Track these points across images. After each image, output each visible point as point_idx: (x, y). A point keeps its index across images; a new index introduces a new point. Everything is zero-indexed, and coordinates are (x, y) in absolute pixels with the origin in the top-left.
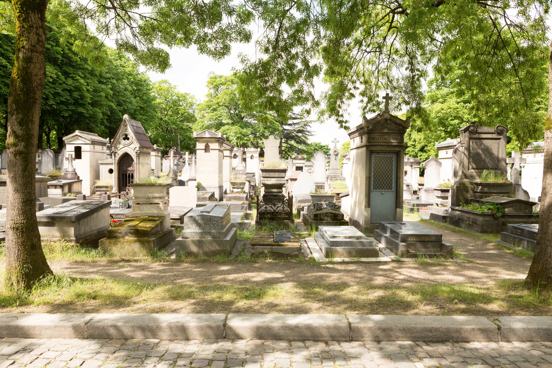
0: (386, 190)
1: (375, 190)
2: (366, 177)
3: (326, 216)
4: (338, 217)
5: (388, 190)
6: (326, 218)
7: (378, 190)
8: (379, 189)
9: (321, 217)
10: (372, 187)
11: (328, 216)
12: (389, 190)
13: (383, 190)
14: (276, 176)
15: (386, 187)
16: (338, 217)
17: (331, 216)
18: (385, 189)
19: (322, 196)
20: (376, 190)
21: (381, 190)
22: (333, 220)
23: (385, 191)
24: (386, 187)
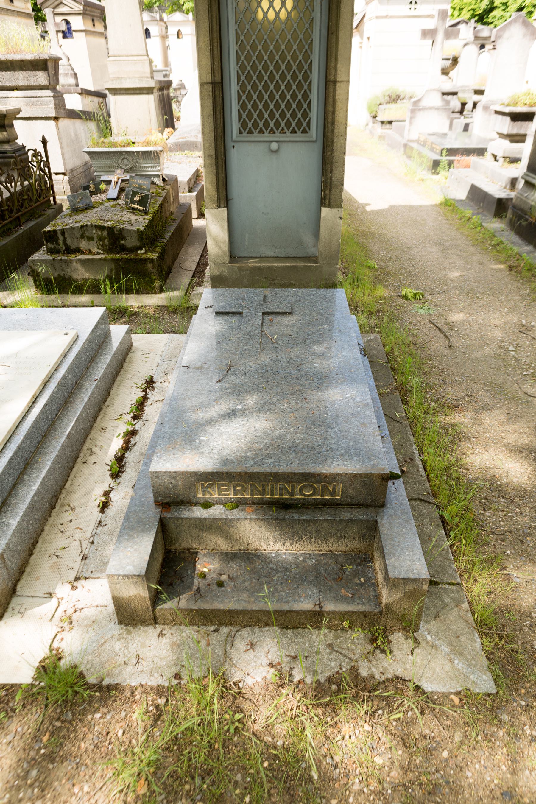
0: (289, 137)
1: (245, 137)
2: (202, 85)
3: (82, 237)
4: (124, 238)
5: (294, 137)
6: (84, 245)
7: (256, 136)
8: (261, 132)
9: (69, 242)
10: (234, 125)
11: (90, 239)
12: (299, 137)
13: (278, 136)
14: (21, 83)
15: (288, 125)
16: (124, 238)
17: (100, 239)
18: (283, 132)
19: (121, 153)
20: (251, 138)
21: (266, 136)
22: (109, 251)
23: (282, 138)
24: (288, 125)
